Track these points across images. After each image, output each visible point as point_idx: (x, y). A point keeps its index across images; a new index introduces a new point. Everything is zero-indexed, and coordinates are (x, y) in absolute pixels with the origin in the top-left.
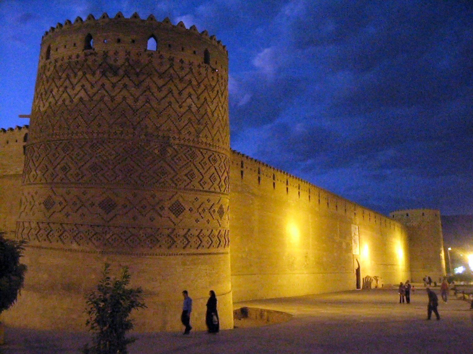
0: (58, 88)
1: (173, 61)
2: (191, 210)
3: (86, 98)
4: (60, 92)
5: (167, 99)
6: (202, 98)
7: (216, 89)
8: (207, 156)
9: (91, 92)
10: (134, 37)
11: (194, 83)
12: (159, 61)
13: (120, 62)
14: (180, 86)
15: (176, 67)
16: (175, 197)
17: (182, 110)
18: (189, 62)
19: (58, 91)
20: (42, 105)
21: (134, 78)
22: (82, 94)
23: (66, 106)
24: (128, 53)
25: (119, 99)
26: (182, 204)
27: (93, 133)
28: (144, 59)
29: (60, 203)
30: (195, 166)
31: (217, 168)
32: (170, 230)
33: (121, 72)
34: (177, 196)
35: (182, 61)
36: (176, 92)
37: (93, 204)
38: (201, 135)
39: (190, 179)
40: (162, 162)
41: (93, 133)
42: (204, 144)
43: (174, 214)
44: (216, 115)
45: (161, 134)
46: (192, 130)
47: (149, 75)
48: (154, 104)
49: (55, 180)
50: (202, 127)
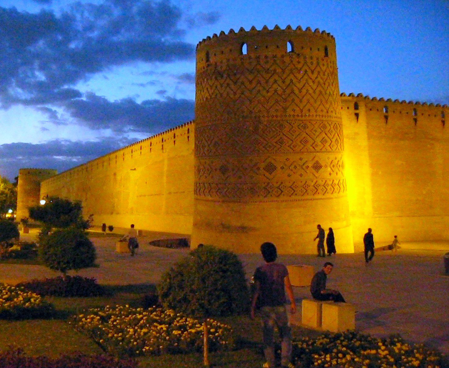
1: (259, 58)
2: (282, 168)
5: (257, 88)
6: (287, 81)
10: (230, 47)
11: (279, 70)
13: (224, 68)
14: (267, 76)
17: (269, 94)
18: (273, 55)
22: (207, 95)
24: (228, 60)
25: (225, 95)
30: (284, 134)
32: (266, 184)
33: (225, 76)
35: (266, 57)
36: (263, 82)
44: (304, 91)
47: (242, 73)
50: (288, 104)
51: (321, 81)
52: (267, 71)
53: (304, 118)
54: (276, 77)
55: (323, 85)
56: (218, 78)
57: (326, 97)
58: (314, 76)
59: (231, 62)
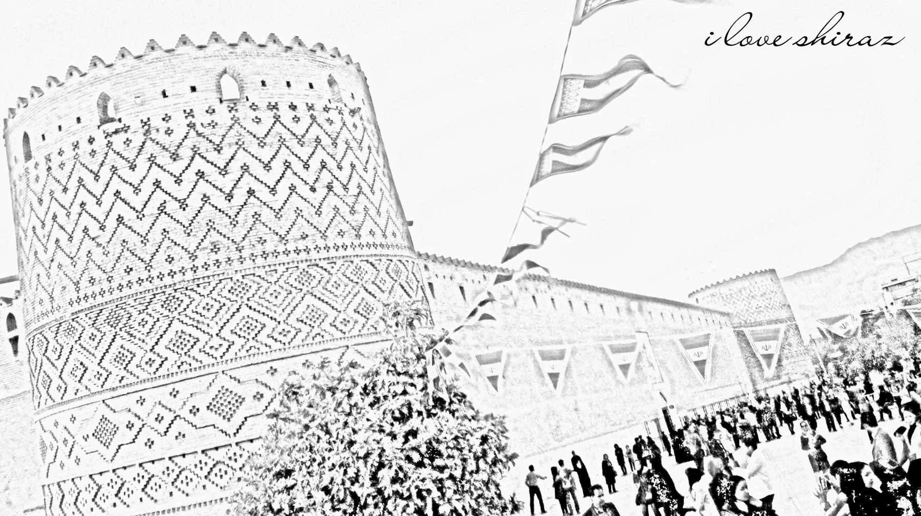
0: (66, 209)
1: (277, 109)
4: (74, 216)
8: (382, 266)
11: (326, 141)
19: (68, 215)
20: (40, 249)
27: (161, 277)
29: (130, 426)
31: (405, 285)
34: (351, 350)
35: (293, 107)
36: (297, 166)
37: (194, 411)
39: (365, 317)
41: (161, 277)
45: (291, 247)
46: (345, 227)
49: (108, 385)
53: (391, 252)
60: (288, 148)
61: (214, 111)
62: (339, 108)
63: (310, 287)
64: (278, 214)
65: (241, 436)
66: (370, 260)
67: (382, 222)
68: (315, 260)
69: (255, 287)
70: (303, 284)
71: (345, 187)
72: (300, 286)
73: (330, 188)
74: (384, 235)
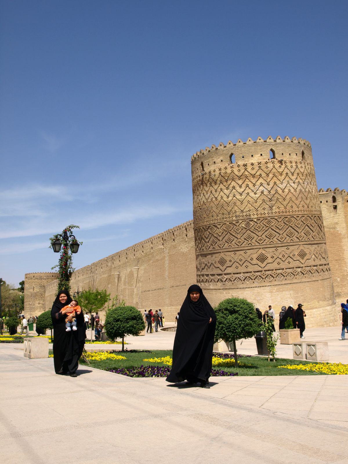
1: (246, 166)
2: (272, 257)
3: (205, 201)
5: (246, 192)
7: (284, 173)
9: (207, 197)
10: (221, 158)
11: (264, 175)
12: (238, 168)
15: (249, 168)
16: (260, 251)
18: (258, 162)
21: (225, 183)
22: (204, 199)
23: (199, 207)
24: (220, 169)
26: (265, 255)
28: (229, 171)
30: (272, 229)
33: (218, 182)
35: (252, 164)
36: (251, 185)
38: (274, 208)
40: (248, 231)
42: (277, 212)
43: (260, 261)
44: (286, 191)
45: (244, 214)
47: (233, 180)
48: (238, 196)
50: (274, 202)
51: (301, 181)
52: (253, 176)
53: (288, 214)
54: (261, 181)
55: (303, 185)
56: (213, 184)
57: (306, 194)
58: (293, 178)
59: (223, 171)
60: (248, 179)
61: (227, 168)
62: (273, 161)
63: (249, 227)
64: (242, 203)
65: (225, 272)
66: (275, 218)
67: (285, 203)
68: (252, 219)
69: (232, 227)
70: (247, 227)
71: (269, 192)
72: (246, 227)
73: (262, 192)
74: (285, 208)
